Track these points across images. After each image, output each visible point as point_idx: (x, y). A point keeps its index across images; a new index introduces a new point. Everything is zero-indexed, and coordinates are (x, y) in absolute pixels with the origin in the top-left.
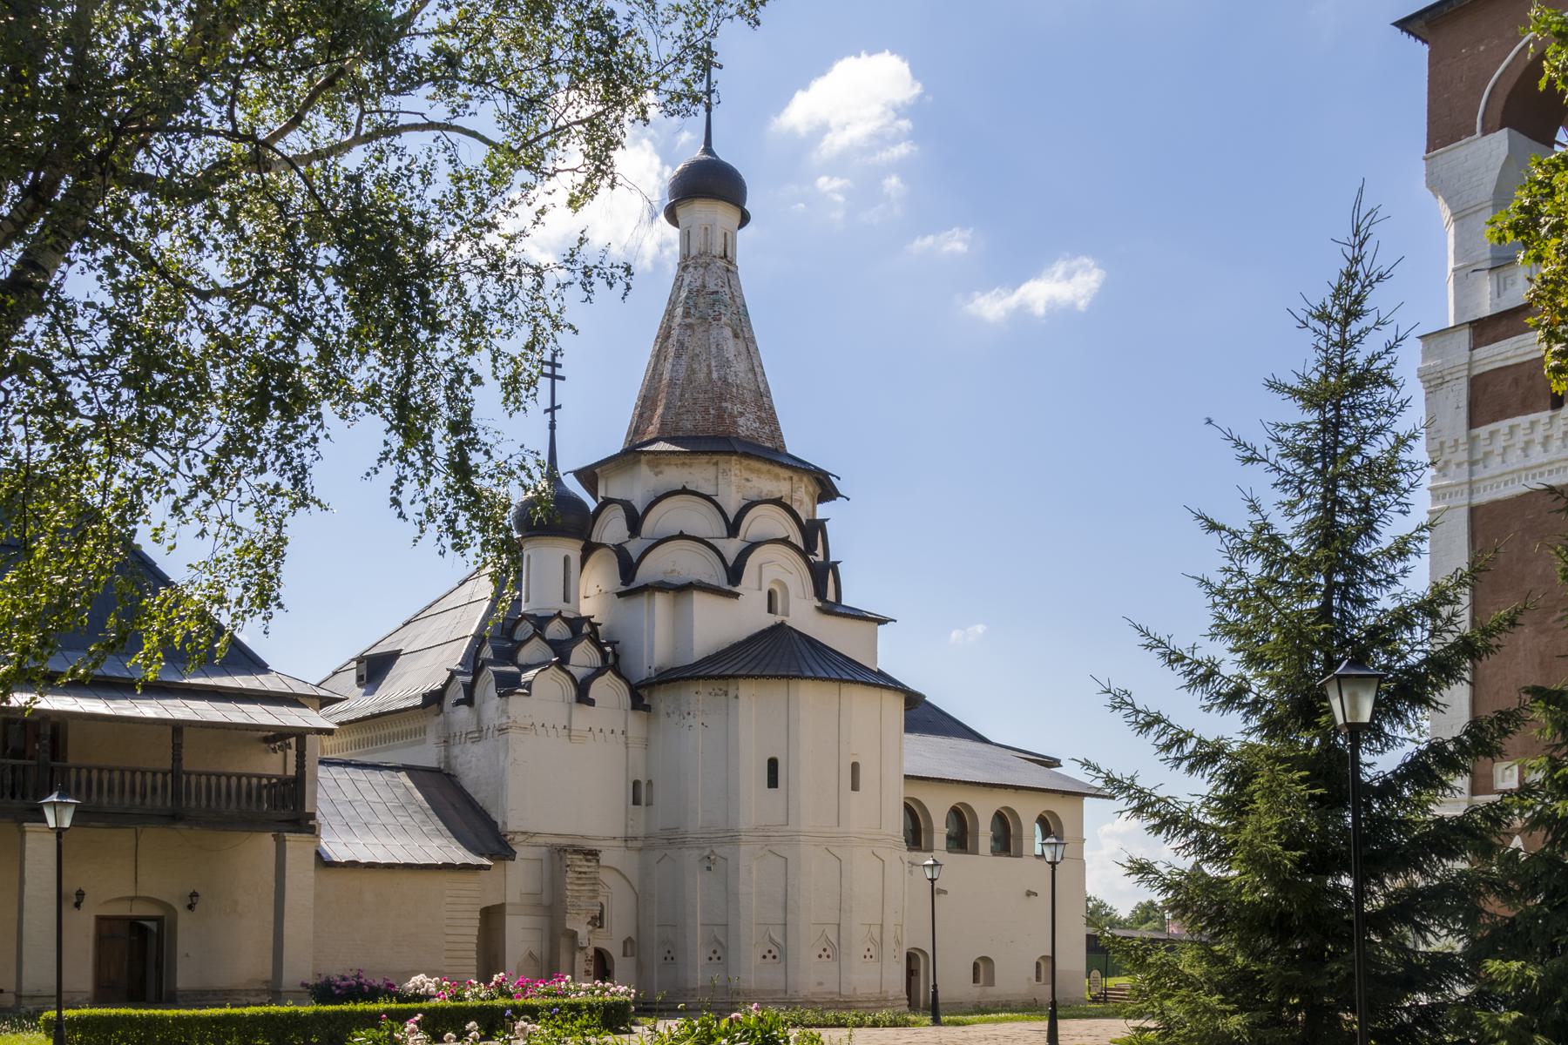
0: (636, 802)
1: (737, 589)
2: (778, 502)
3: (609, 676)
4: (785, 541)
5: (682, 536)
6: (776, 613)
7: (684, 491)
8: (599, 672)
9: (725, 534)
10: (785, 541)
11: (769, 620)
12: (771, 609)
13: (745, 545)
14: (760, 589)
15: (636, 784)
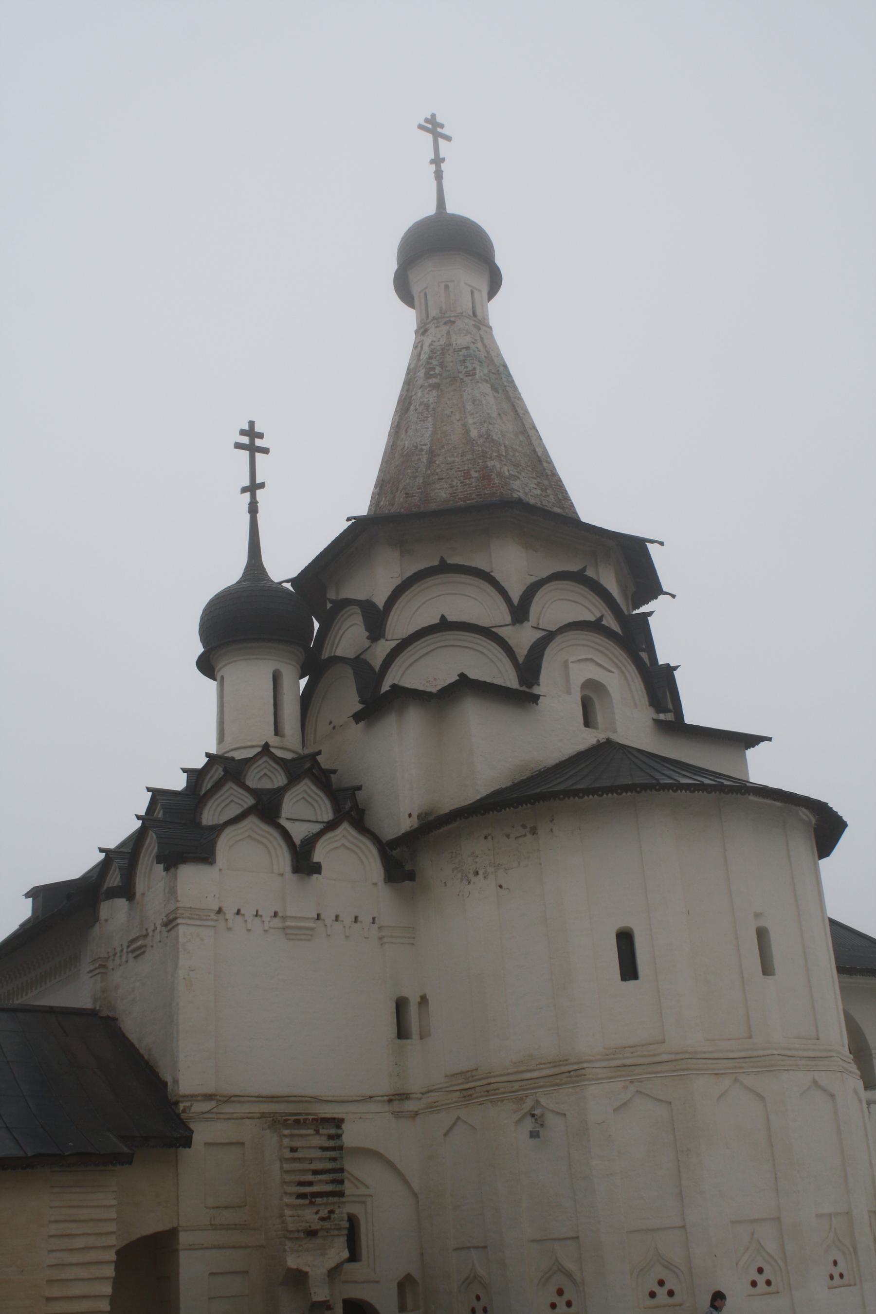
0: (402, 1032)
1: (536, 690)
2: (579, 578)
3: (345, 830)
4: (595, 627)
5: (444, 625)
6: (595, 727)
7: (444, 568)
8: (330, 826)
9: (508, 619)
10: (595, 627)
11: (588, 738)
12: (588, 723)
13: (539, 634)
14: (569, 692)
15: (401, 1005)
